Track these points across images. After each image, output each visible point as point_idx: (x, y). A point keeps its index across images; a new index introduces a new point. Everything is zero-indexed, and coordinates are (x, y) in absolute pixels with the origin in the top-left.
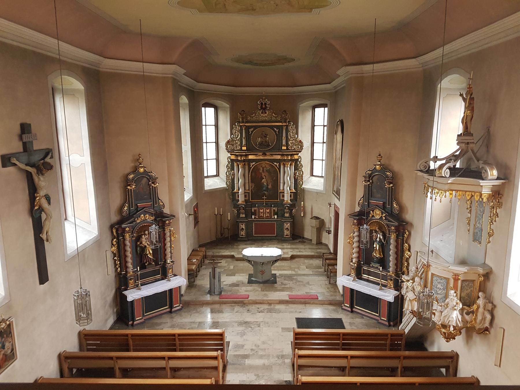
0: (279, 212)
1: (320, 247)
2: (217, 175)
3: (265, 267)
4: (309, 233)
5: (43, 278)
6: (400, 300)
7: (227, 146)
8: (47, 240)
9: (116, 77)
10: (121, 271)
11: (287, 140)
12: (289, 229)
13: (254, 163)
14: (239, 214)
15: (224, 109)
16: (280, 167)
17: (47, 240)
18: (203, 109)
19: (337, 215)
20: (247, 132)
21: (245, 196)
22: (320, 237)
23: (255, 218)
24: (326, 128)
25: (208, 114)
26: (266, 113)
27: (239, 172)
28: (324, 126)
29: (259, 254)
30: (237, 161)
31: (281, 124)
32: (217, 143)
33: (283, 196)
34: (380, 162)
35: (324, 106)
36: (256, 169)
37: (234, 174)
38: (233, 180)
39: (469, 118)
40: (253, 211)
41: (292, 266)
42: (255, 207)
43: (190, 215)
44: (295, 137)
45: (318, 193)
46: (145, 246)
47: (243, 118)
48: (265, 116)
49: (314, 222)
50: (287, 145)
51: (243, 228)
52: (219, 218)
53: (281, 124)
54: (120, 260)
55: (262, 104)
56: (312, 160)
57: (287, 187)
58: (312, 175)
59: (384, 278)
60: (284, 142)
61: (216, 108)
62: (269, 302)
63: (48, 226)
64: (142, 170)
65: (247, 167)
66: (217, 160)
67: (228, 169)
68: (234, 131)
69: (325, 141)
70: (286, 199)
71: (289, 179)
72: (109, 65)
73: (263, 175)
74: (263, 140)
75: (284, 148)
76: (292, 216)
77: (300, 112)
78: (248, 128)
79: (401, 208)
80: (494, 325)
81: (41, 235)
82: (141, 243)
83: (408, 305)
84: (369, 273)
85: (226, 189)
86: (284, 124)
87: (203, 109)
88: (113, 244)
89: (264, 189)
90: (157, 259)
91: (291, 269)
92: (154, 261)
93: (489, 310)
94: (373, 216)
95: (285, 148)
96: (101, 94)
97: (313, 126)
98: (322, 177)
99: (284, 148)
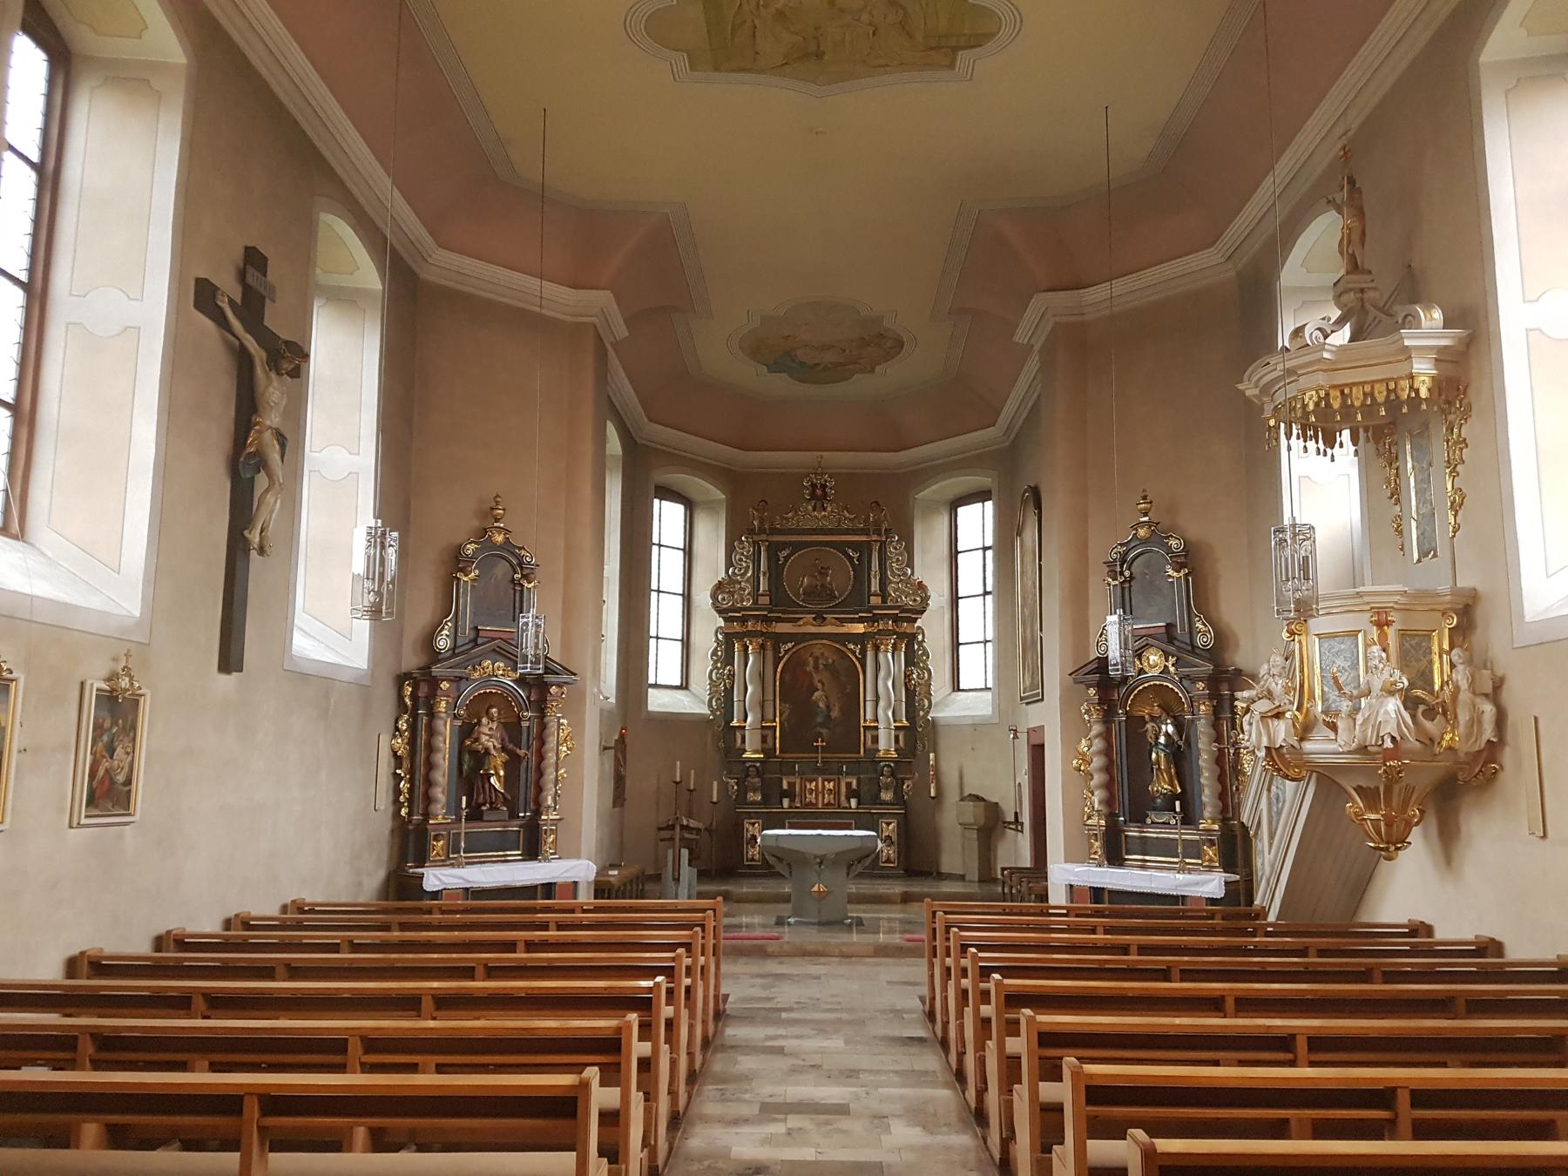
2: (685, 686)
4: (956, 853)
5: (230, 660)
6: (1241, 893)
7: (714, 596)
8: (262, 551)
9: (456, 300)
10: (410, 814)
11: (883, 583)
12: (894, 838)
15: (710, 506)
16: (864, 656)
17: (262, 551)
18: (656, 501)
19: (1037, 752)
21: (764, 739)
24: (989, 553)
25: (668, 518)
27: (749, 666)
28: (985, 549)
30: (740, 636)
31: (864, 538)
32: (687, 597)
33: (875, 740)
34: (1146, 515)
35: (981, 496)
37: (731, 676)
38: (729, 692)
39: (1356, 237)
40: (785, 786)
43: (605, 748)
44: (905, 574)
45: (978, 727)
46: (487, 750)
47: (762, 521)
48: (826, 516)
52: (685, 796)
53: (864, 538)
54: (411, 781)
55: (814, 486)
56: (956, 645)
58: (956, 688)
59: (1193, 849)
60: (875, 587)
61: (690, 506)
62: (844, 949)
63: (270, 510)
64: (499, 538)
65: (770, 654)
67: (716, 662)
68: (735, 557)
69: (989, 588)
70: (882, 745)
71: (890, 684)
72: (446, 265)
74: (820, 582)
75: (875, 600)
76: (899, 799)
77: (917, 513)
78: (773, 550)
79: (1222, 639)
80: (1509, 737)
81: (246, 533)
82: (477, 740)
83: (1259, 734)
84: (1146, 846)
86: (875, 537)
87: (656, 501)
88: (397, 729)
89: (819, 720)
90: (515, 797)
92: (506, 802)
93: (1486, 695)
94: (1141, 671)
96: (418, 324)
97: (954, 553)
98: (987, 689)
99: (875, 600)
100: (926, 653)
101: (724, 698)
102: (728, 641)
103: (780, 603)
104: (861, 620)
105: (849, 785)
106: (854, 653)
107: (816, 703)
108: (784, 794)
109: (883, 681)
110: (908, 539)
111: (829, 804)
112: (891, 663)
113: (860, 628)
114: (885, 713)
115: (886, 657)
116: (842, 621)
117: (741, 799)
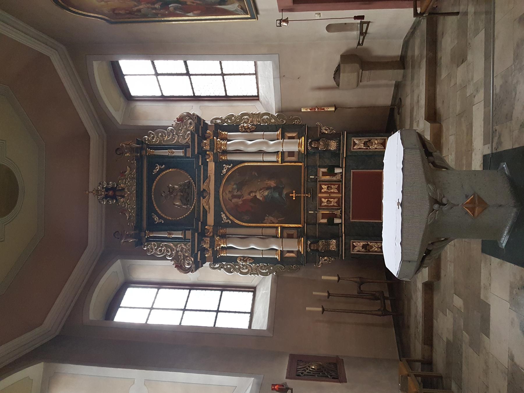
0: (328, 162)
1: (409, 59)
2: (253, 289)
3: (456, 194)
4: (377, 92)
7: (186, 271)
12: (365, 139)
13: (223, 216)
14: (328, 253)
15: (127, 270)
20: (159, 228)
21: (290, 236)
22: (387, 63)
23: (341, 218)
26: (123, 189)
27: (238, 247)
29: (90, 308)
30: (215, 253)
33: (291, 154)
35: (118, 77)
36: (237, 212)
37: (244, 259)
38: (256, 260)
40: (325, 221)
41: (458, 108)
42: (315, 216)
45: (282, 75)
49: (346, 77)
50: (178, 147)
51: (364, 247)
55: (106, 197)
56: (226, 98)
57: (266, 143)
58: (256, 98)
60: (179, 153)
61: (128, 283)
65: (229, 230)
66: (223, 288)
67: (235, 270)
70: (294, 148)
73: (249, 197)
78: (153, 227)
85: (277, 276)
89: (276, 195)
91: (466, 114)
95: (189, 150)
100: (230, 117)
101: (259, 264)
102: (218, 260)
103: (193, 224)
104: (205, 164)
105: (324, 174)
106: (229, 170)
107: (265, 197)
108: (331, 222)
109: (244, 146)
110: (147, 129)
111: (338, 189)
112: (236, 141)
113: (212, 166)
114: (273, 146)
115: (231, 145)
116: (206, 177)
117: (335, 254)
